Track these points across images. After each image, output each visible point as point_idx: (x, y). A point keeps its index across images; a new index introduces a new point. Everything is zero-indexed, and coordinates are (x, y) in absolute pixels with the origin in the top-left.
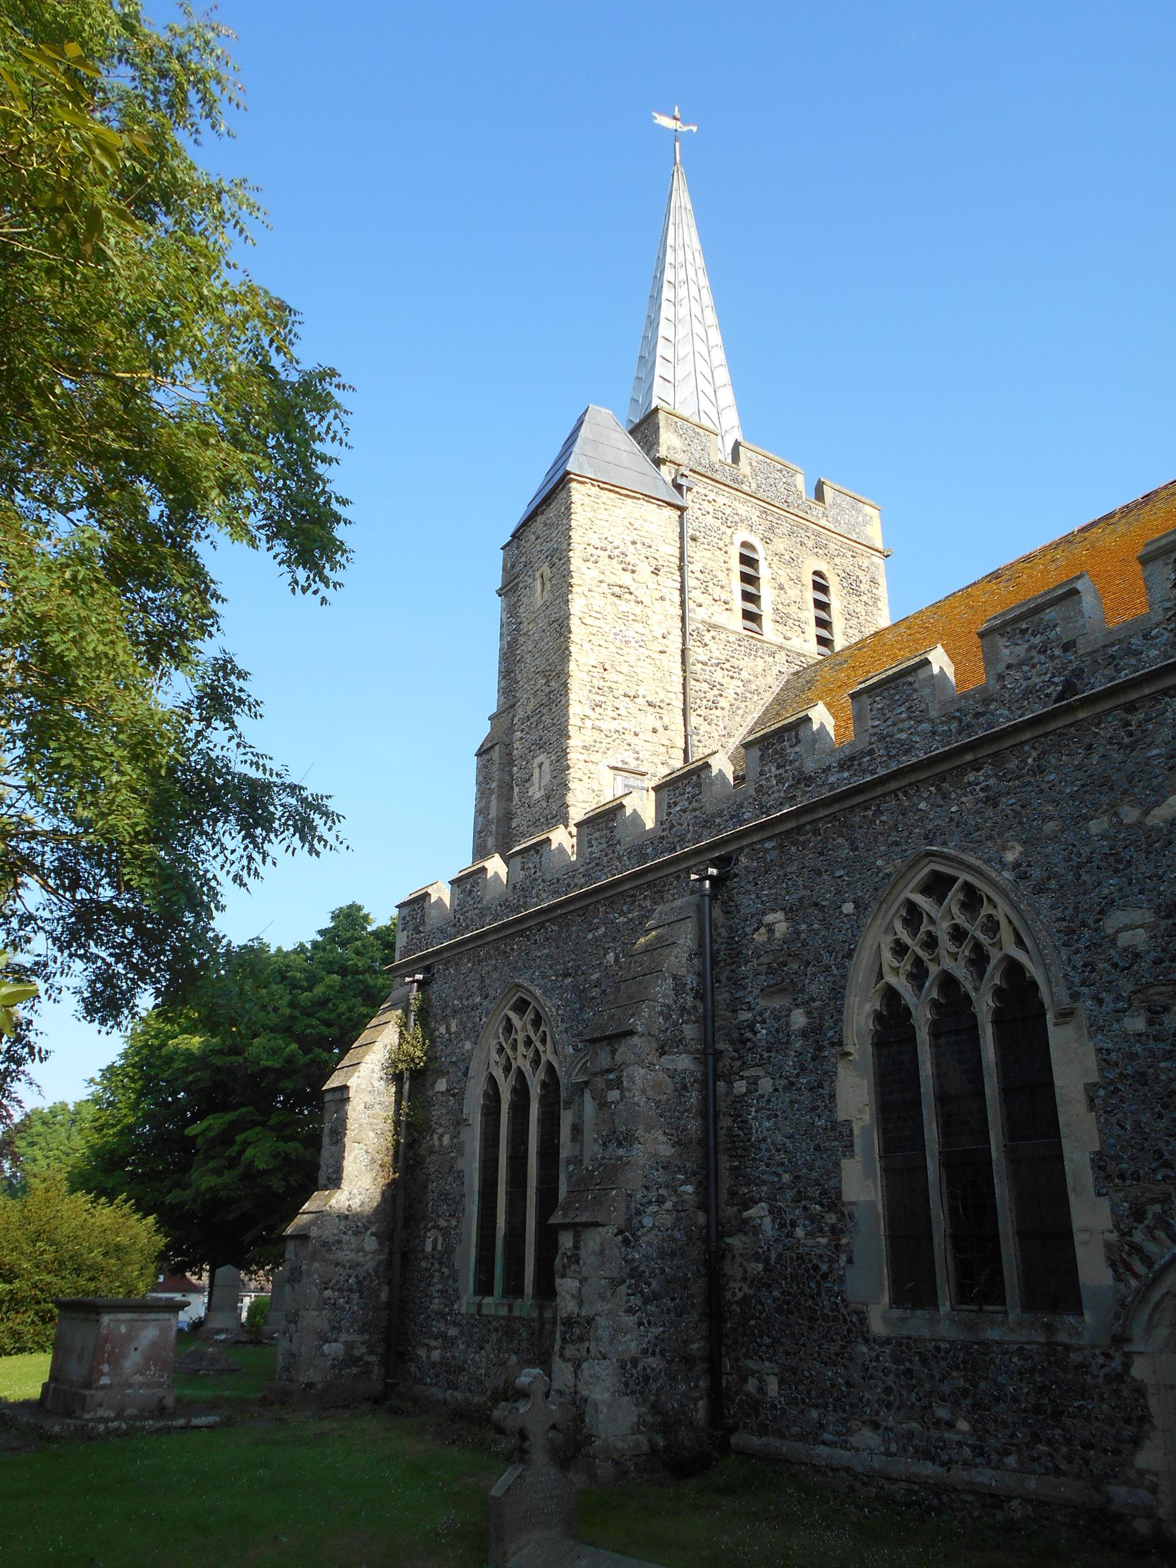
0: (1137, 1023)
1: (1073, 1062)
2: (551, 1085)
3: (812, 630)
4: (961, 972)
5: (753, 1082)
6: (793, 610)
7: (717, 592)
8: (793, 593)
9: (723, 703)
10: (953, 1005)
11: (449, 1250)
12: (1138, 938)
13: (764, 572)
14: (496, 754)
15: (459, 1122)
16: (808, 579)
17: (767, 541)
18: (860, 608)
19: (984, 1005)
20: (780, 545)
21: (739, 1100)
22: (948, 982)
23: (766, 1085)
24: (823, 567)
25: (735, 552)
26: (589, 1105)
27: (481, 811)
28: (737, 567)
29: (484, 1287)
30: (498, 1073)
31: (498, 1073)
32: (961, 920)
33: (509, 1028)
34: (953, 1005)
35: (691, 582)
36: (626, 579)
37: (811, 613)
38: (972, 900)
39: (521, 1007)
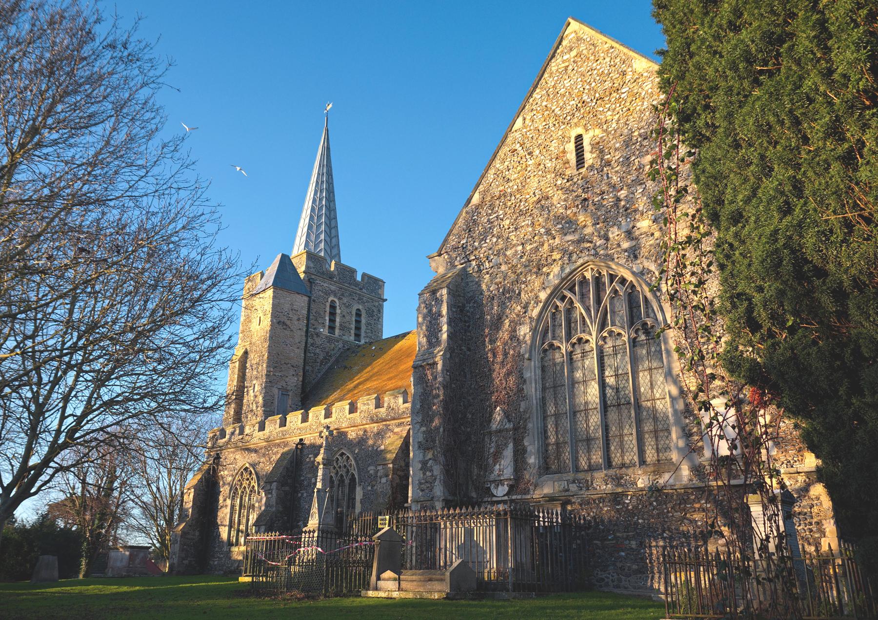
0: (369, 488)
1: (359, 494)
3: (353, 332)
4: (344, 475)
5: (302, 494)
6: (347, 325)
8: (348, 318)
9: (318, 360)
12: (371, 472)
16: (354, 312)
17: (340, 299)
18: (372, 322)
19: (347, 481)
20: (345, 300)
21: (300, 498)
22: (342, 476)
23: (305, 495)
24: (360, 307)
25: (328, 305)
28: (328, 309)
35: (311, 317)
37: (353, 326)
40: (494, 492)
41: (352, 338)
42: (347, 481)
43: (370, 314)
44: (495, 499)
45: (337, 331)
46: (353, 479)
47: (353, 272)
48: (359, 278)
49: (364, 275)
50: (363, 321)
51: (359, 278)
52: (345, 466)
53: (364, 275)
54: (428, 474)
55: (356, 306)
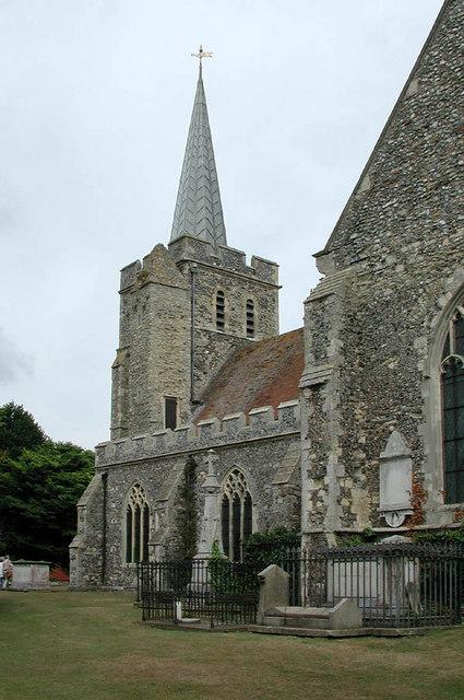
0: (266, 508)
2: (147, 509)
3: (245, 327)
7: (207, 315)
10: (237, 501)
11: (118, 551)
13: (226, 303)
14: (120, 369)
15: (120, 517)
24: (252, 297)
26: (157, 517)
27: (115, 392)
28: (215, 302)
29: (129, 560)
30: (131, 504)
31: (131, 504)
32: (240, 481)
33: (134, 492)
34: (237, 501)
36: (171, 322)
37: (245, 319)
38: (242, 477)
39: (137, 486)
40: (388, 522)
41: (245, 334)
42: (243, 501)
43: (264, 305)
44: (390, 529)
45: (226, 326)
46: (248, 499)
47: (241, 255)
48: (248, 263)
49: (254, 258)
50: (255, 312)
51: (248, 263)
52: (239, 484)
53: (254, 258)
54: (319, 504)
55: (246, 296)
